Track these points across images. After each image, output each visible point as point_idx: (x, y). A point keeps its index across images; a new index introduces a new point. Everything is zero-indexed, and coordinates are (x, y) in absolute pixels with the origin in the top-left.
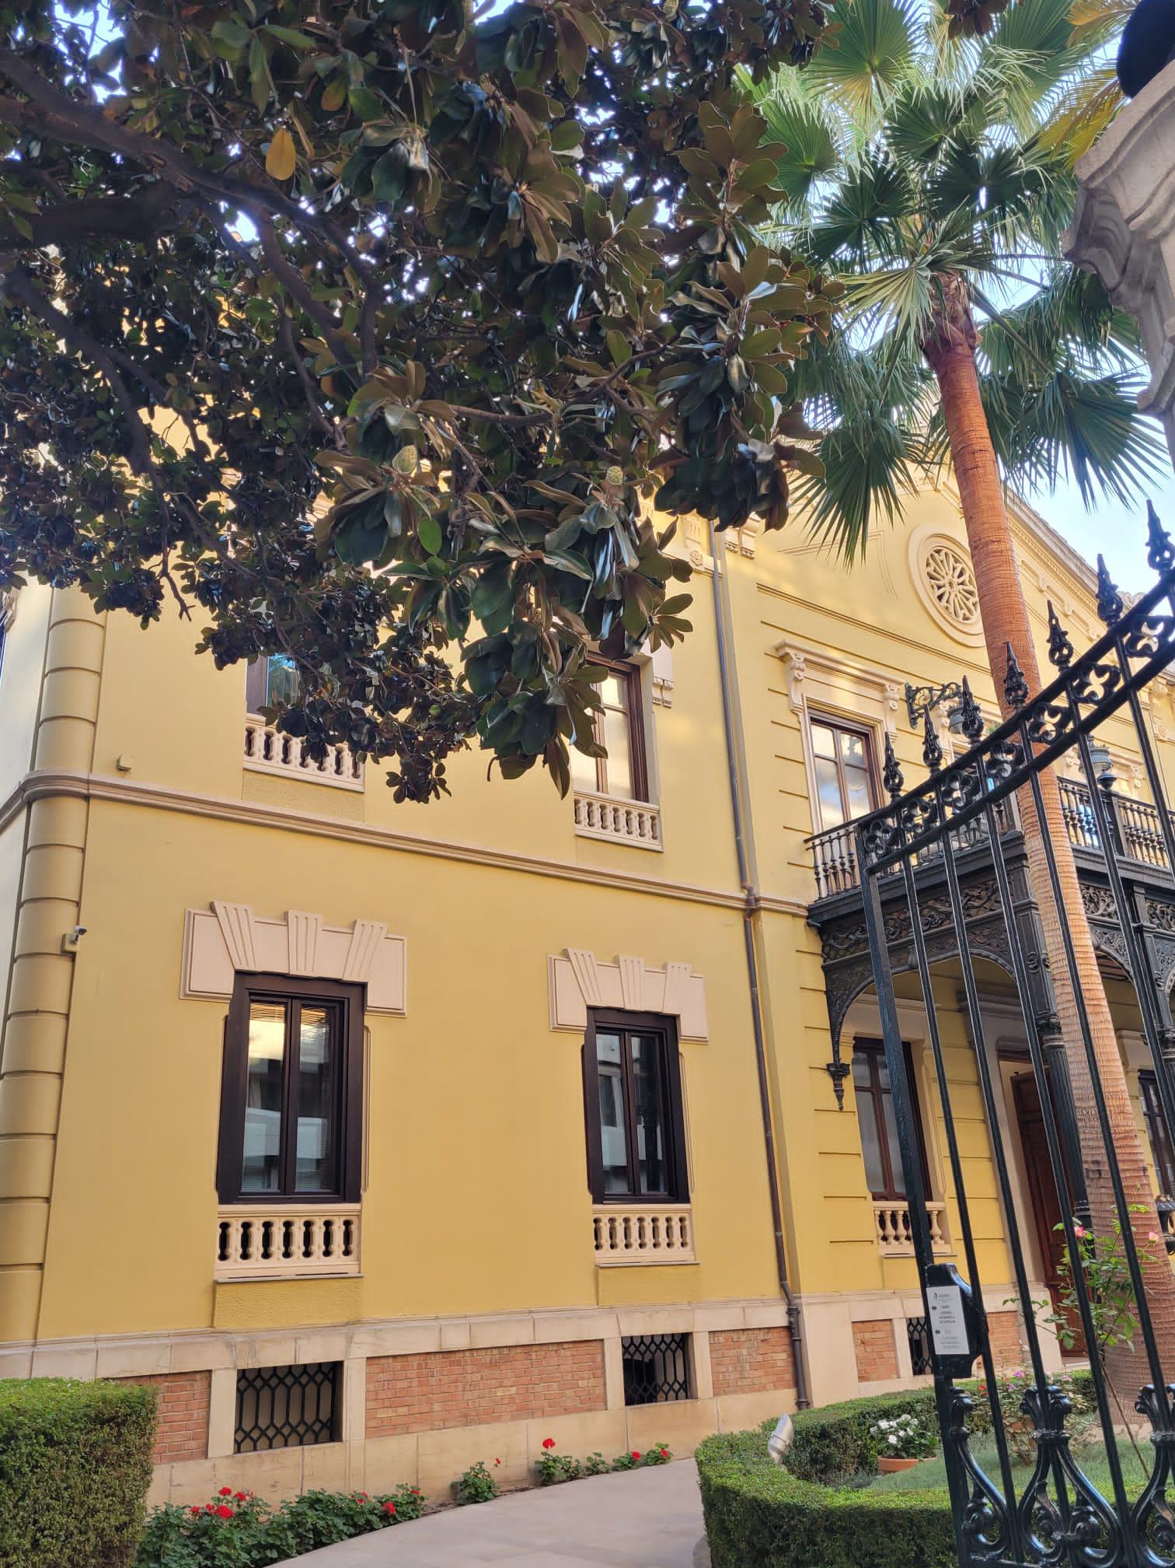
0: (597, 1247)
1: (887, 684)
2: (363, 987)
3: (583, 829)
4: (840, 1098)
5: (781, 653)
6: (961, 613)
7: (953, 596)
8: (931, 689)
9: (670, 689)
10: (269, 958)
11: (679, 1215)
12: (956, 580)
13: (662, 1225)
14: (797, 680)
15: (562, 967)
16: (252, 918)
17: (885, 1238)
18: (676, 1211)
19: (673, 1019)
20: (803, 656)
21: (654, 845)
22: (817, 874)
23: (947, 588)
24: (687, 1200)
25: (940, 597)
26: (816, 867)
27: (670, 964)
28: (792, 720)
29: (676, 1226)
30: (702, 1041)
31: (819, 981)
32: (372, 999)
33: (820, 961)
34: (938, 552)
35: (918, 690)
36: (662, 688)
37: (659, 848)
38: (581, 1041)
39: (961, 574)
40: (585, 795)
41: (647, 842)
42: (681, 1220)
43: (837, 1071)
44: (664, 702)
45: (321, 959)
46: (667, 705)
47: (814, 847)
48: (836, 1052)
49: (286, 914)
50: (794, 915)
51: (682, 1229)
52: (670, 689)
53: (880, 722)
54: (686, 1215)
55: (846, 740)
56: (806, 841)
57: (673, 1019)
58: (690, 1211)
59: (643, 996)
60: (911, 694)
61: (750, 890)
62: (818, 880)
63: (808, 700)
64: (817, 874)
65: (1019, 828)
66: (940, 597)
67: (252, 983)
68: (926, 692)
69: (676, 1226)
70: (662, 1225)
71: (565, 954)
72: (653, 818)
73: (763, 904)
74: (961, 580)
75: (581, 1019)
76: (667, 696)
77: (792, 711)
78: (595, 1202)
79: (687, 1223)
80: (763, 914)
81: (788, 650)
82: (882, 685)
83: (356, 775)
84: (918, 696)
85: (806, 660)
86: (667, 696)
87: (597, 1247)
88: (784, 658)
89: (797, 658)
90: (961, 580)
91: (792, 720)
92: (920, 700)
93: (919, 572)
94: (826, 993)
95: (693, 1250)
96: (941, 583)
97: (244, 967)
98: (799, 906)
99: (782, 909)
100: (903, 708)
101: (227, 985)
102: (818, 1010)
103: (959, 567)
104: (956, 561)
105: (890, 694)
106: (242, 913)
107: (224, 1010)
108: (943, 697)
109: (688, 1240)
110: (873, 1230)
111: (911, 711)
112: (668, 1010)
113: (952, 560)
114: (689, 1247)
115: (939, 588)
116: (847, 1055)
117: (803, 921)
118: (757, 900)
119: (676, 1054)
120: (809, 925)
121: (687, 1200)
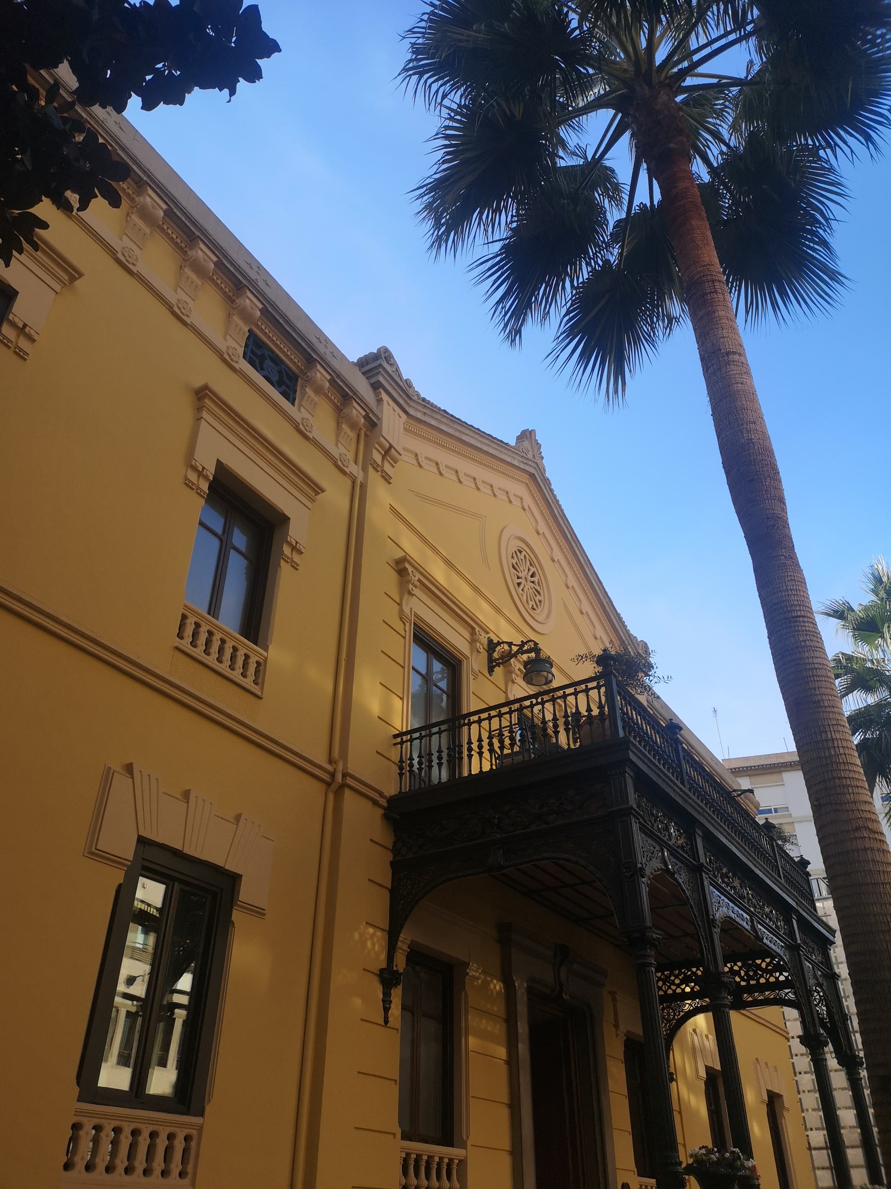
0: (67, 1166)
1: (477, 629)
3: (185, 644)
4: (386, 1010)
5: (401, 566)
6: (531, 603)
7: (526, 589)
8: (510, 644)
9: (300, 552)
11: (186, 1132)
12: (529, 578)
13: (162, 1143)
14: (410, 593)
18: (183, 1125)
19: (234, 879)
20: (418, 576)
21: (256, 689)
22: (401, 768)
24: (201, 1113)
25: (519, 584)
28: (399, 626)
29: (179, 1145)
30: (258, 912)
31: (386, 879)
33: (390, 857)
34: (520, 552)
35: (499, 643)
36: (293, 548)
37: (259, 694)
38: (119, 876)
39: (532, 576)
41: (248, 682)
42: (188, 1139)
43: (388, 978)
44: (292, 561)
46: (295, 566)
47: (402, 743)
50: (375, 803)
51: (186, 1151)
52: (300, 552)
53: (467, 658)
54: (194, 1132)
55: (437, 666)
56: (395, 736)
57: (234, 879)
58: (200, 1129)
62: (401, 775)
63: (416, 616)
65: (621, 734)
66: (519, 584)
68: (506, 647)
69: (179, 1145)
70: (162, 1143)
71: (129, 769)
72: (257, 662)
73: (349, 781)
74: (533, 579)
75: (128, 850)
76: (296, 558)
77: (401, 619)
78: (80, 1099)
79: (193, 1144)
81: (407, 565)
82: (473, 628)
84: (499, 648)
85: (419, 580)
86: (296, 558)
87: (67, 1166)
88: (402, 572)
89: (416, 577)
90: (533, 579)
94: (392, 891)
95: (193, 1184)
96: (520, 575)
98: (381, 794)
100: (484, 655)
102: (379, 905)
103: (533, 570)
104: (531, 565)
108: (521, 651)
109: (190, 1169)
111: (490, 660)
113: (528, 562)
114: (186, 1181)
115: (518, 578)
116: (400, 963)
117: (381, 811)
119: (229, 923)
120: (387, 817)
121: (201, 1113)
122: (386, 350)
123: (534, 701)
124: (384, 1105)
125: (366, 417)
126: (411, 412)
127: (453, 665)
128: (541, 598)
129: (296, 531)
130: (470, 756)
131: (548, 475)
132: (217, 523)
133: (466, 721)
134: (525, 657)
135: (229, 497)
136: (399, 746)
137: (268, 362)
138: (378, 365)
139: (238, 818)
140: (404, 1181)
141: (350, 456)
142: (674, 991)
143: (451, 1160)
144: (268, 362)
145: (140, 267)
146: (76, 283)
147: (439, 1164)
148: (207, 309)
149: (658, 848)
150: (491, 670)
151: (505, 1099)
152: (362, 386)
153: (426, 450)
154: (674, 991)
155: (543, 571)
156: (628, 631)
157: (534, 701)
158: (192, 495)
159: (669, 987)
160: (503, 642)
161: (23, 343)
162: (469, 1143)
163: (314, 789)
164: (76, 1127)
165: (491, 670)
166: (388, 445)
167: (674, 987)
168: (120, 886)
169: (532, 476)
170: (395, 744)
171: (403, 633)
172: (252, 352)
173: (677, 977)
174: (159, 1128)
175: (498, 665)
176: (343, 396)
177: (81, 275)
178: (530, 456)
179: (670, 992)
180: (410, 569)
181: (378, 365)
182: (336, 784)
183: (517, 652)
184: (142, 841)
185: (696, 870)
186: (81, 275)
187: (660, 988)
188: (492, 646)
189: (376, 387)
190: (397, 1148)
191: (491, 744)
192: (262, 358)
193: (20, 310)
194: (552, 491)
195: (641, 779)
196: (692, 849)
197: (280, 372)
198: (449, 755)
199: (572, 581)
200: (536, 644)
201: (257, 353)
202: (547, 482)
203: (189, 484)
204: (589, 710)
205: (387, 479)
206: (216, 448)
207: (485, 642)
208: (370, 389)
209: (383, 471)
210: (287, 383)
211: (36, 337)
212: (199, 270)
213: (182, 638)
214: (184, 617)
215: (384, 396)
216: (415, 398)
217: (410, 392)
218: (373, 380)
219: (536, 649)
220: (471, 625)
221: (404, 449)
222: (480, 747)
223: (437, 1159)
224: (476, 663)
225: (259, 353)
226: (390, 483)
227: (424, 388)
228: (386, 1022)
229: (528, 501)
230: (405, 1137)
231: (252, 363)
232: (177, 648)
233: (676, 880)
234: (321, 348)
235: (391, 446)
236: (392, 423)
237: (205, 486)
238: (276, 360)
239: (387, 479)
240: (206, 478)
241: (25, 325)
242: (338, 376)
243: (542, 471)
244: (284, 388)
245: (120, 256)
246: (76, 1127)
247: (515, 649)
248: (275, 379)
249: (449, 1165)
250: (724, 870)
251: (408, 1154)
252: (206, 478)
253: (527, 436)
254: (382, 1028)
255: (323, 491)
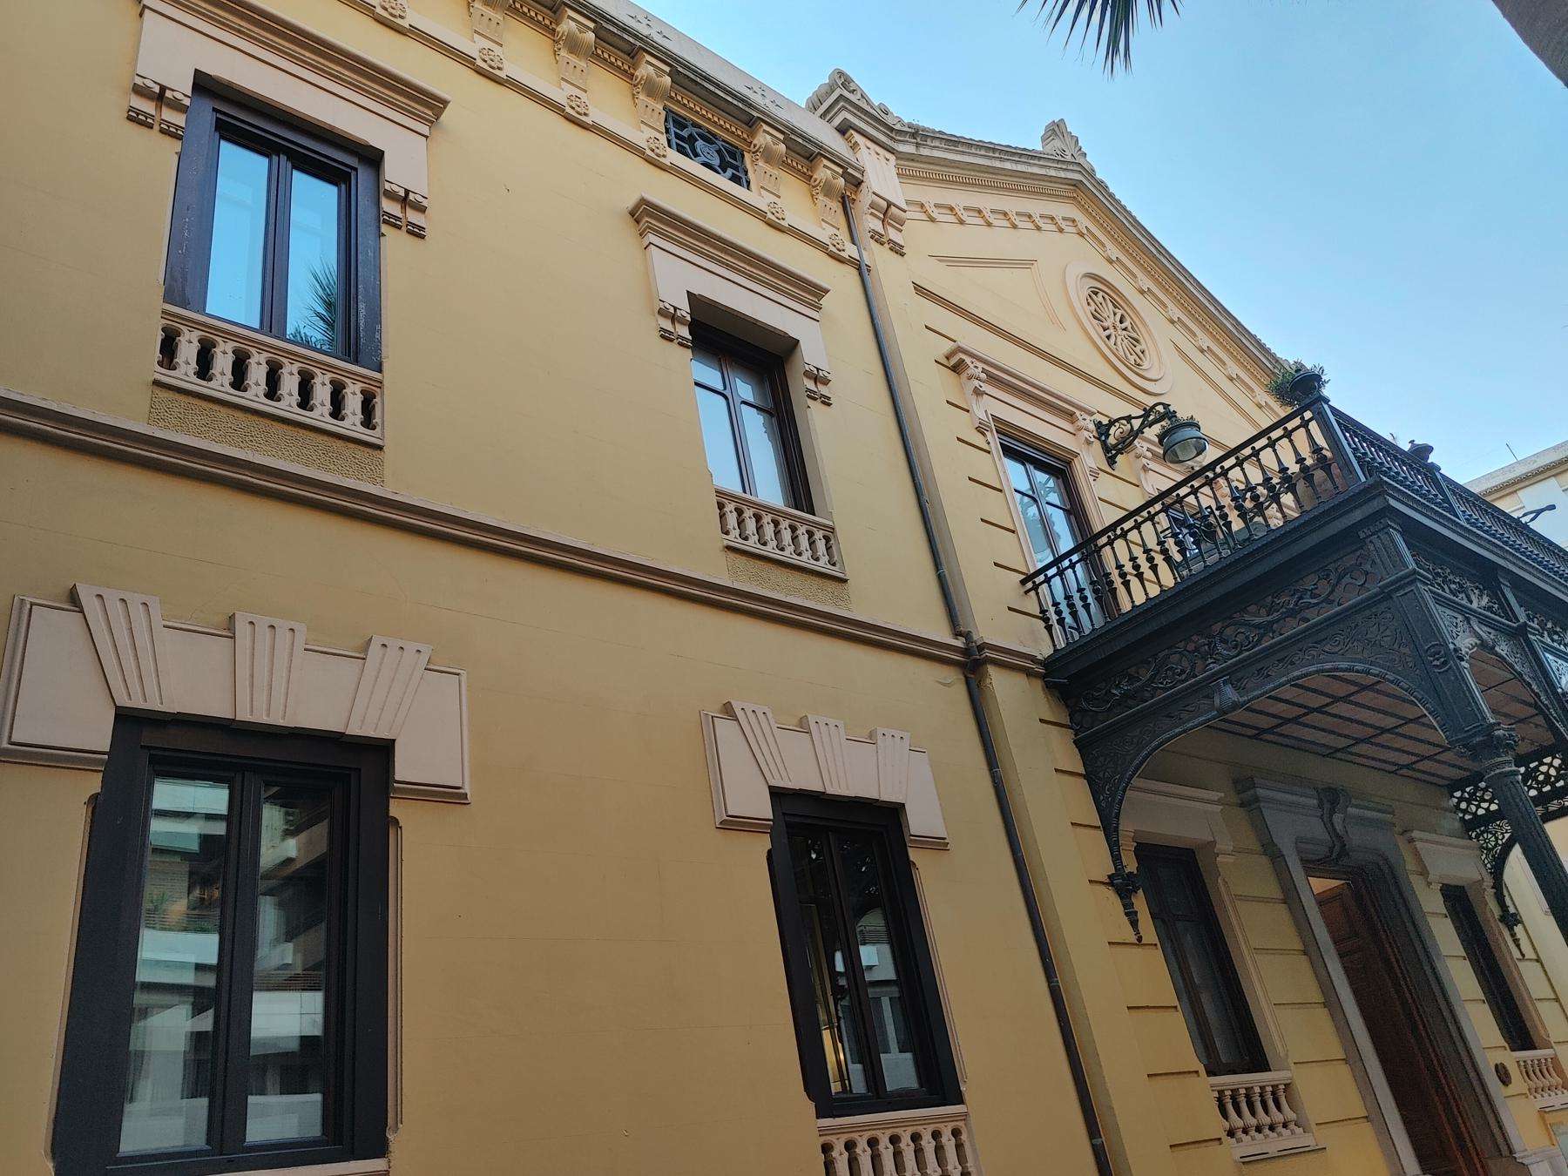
1: (1078, 413)
2: (383, 750)
4: (1134, 924)
5: (953, 361)
8: (1129, 418)
10: (191, 683)
13: (928, 1144)
15: (725, 728)
16: (158, 622)
17: (1231, 1133)
20: (981, 365)
23: (1111, 331)
24: (961, 1101)
25: (1108, 337)
26: (1043, 611)
27: (880, 731)
28: (978, 440)
30: (938, 845)
32: (405, 769)
35: (1112, 423)
40: (732, 497)
41: (822, 565)
42: (956, 1133)
43: (1122, 885)
45: (308, 696)
47: (1036, 588)
48: (1117, 859)
49: (232, 618)
50: (1029, 673)
51: (959, 1147)
55: (1041, 477)
56: (1023, 582)
59: (851, 774)
60: (1103, 430)
61: (967, 636)
62: (1049, 628)
64: (1046, 620)
66: (1108, 337)
67: (151, 737)
70: (928, 1144)
71: (728, 711)
79: (964, 1137)
80: (992, 670)
83: (368, 422)
84: (1113, 430)
86: (823, 390)
88: (957, 368)
89: (976, 368)
91: (978, 440)
92: (1112, 441)
93: (1084, 312)
97: (137, 702)
98: (1033, 659)
99: (1015, 662)
100: (1097, 445)
101: (98, 735)
102: (1080, 801)
105: (1081, 423)
106: (137, 611)
107: (94, 783)
108: (1146, 423)
110: (1217, 1126)
111: (1106, 448)
112: (888, 795)
116: (1131, 865)
118: (982, 647)
119: (909, 865)
120: (1049, 687)
122: (841, 74)
123: (1211, 475)
124: (1173, 1038)
125: (845, 175)
126: (901, 148)
127: (1059, 467)
128: (1143, 347)
129: (812, 352)
130: (1126, 584)
131: (1099, 176)
132: (712, 377)
133: (1119, 532)
134: (1157, 429)
135: (718, 337)
136: (1033, 593)
137: (700, 144)
138: (840, 98)
139: (872, 735)
140: (1227, 1125)
141: (843, 235)
142: (1487, 809)
143: (1275, 1087)
144: (700, 144)
145: (509, 70)
146: (442, 118)
147: (1261, 1095)
148: (607, 99)
149: (1460, 618)
150: (1111, 461)
151: (1317, 997)
152: (824, 134)
153: (933, 195)
154: (1487, 809)
155: (1133, 309)
156: (1273, 356)
157: (1211, 475)
158: (674, 346)
159: (1478, 807)
160: (1117, 420)
161: (413, 217)
162: (1291, 1062)
163: (953, 676)
164: (826, 1149)
165: (1111, 461)
166: (884, 204)
167: (1485, 805)
168: (769, 852)
169: (1076, 185)
170: (1027, 592)
171: (986, 447)
172: (677, 136)
173: (1485, 790)
174: (920, 1129)
175: (1120, 452)
176: (803, 155)
177: (445, 103)
178: (1069, 158)
179: (1481, 812)
180: (968, 360)
181: (840, 98)
182: (973, 662)
183: (1143, 426)
184: (777, 794)
185: (1518, 634)
186: (445, 103)
187: (1465, 811)
188: (1103, 430)
189: (843, 130)
190: (1205, 1088)
191: (1165, 552)
192: (691, 140)
193: (396, 173)
194: (1111, 195)
195: (1412, 531)
196: (1501, 606)
197: (719, 152)
198: (1095, 591)
199: (1176, 312)
200: (1166, 406)
201: (684, 135)
202: (1101, 185)
203: (666, 336)
204: (1300, 460)
205: (898, 250)
206: (680, 278)
207: (1092, 427)
208: (837, 135)
209: (890, 241)
210: (731, 162)
211: (425, 203)
212: (574, 46)
213: (727, 533)
214: (721, 506)
215: (857, 137)
216: (898, 127)
217: (890, 121)
218: (837, 121)
219: (1169, 414)
220: (1066, 411)
221: (908, 202)
222: (1150, 560)
223: (1257, 1090)
224: (1089, 458)
225: (685, 133)
226: (902, 255)
227: (905, 112)
228: (1140, 939)
229: (1084, 222)
230: (1210, 1073)
231: (681, 150)
232: (728, 548)
233: (1497, 654)
234: (756, 99)
235: (889, 204)
236: (881, 175)
237: (684, 332)
238: (709, 139)
239: (898, 250)
240: (682, 321)
241: (407, 192)
242: (793, 131)
243: (1090, 173)
244: (730, 171)
245: (480, 63)
246: (826, 1149)
247: (1136, 424)
248: (716, 162)
249: (1273, 1093)
250: (1549, 625)
251: (1221, 1092)
252: (682, 321)
253: (1056, 130)
254: (1135, 951)
255: (827, 291)
